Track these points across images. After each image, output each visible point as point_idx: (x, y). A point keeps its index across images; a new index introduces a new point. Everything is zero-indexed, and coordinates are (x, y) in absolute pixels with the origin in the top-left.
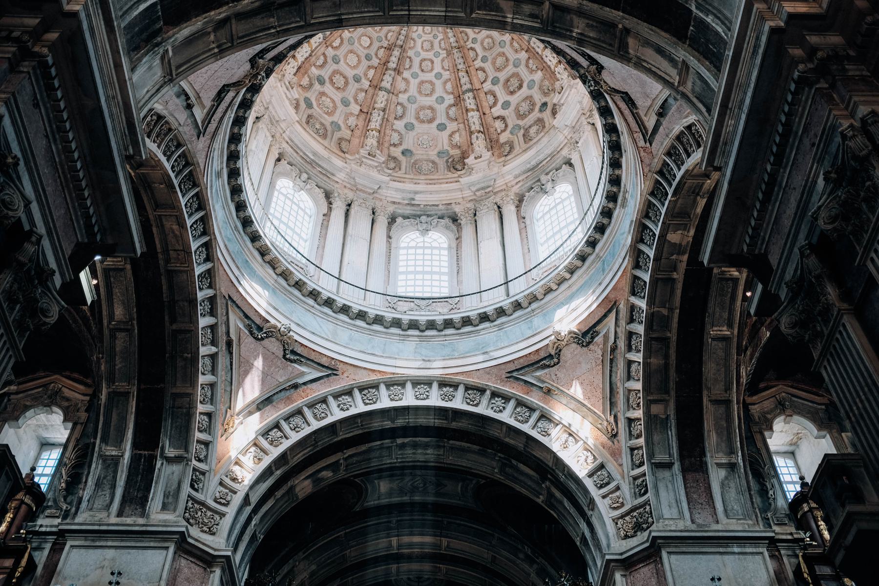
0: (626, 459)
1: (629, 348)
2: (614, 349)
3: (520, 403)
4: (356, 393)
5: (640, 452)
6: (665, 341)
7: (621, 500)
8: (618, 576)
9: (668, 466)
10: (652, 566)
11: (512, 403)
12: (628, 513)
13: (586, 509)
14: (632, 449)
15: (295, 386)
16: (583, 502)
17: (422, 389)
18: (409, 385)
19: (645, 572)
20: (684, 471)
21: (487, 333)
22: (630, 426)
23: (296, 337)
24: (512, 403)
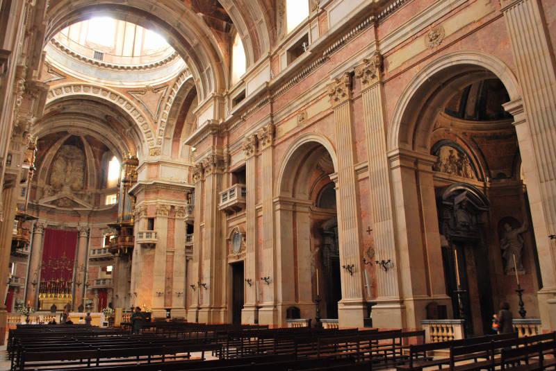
1: (168, 101)
2: (163, 98)
3: (128, 103)
4: (72, 87)
6: (179, 104)
11: (126, 103)
14: (160, 130)
15: (50, 81)
16: (142, 140)
17: (96, 90)
18: (92, 88)
19: (154, 168)
20: (173, 141)
21: (123, 74)
23: (54, 65)
24: (126, 103)
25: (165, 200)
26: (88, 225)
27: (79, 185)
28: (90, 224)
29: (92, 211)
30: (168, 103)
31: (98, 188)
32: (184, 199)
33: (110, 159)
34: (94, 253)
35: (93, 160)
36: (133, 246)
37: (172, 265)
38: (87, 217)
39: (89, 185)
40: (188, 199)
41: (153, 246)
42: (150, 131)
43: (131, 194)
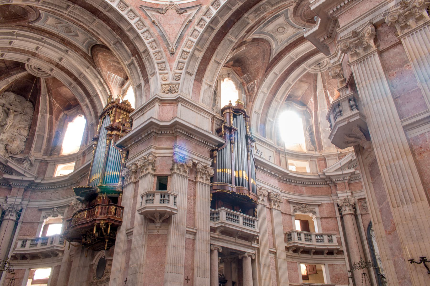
0: (175, 64)
5: (183, 65)
7: (167, 78)
8: (157, 104)
9: (191, 75)
10: (173, 106)
12: (167, 84)
13: (149, 75)
14: (179, 62)
20: (195, 80)
22: (182, 53)
25: (184, 151)
26: (21, 203)
27: (18, 147)
28: (25, 202)
29: (31, 183)
30: (198, 28)
31: (45, 153)
32: (208, 156)
33: (71, 120)
34: (23, 246)
35: (48, 116)
36: (121, 222)
37: (193, 255)
38: (23, 190)
39: (33, 148)
40: (212, 156)
41: (166, 218)
42: (164, 62)
43: (120, 146)
